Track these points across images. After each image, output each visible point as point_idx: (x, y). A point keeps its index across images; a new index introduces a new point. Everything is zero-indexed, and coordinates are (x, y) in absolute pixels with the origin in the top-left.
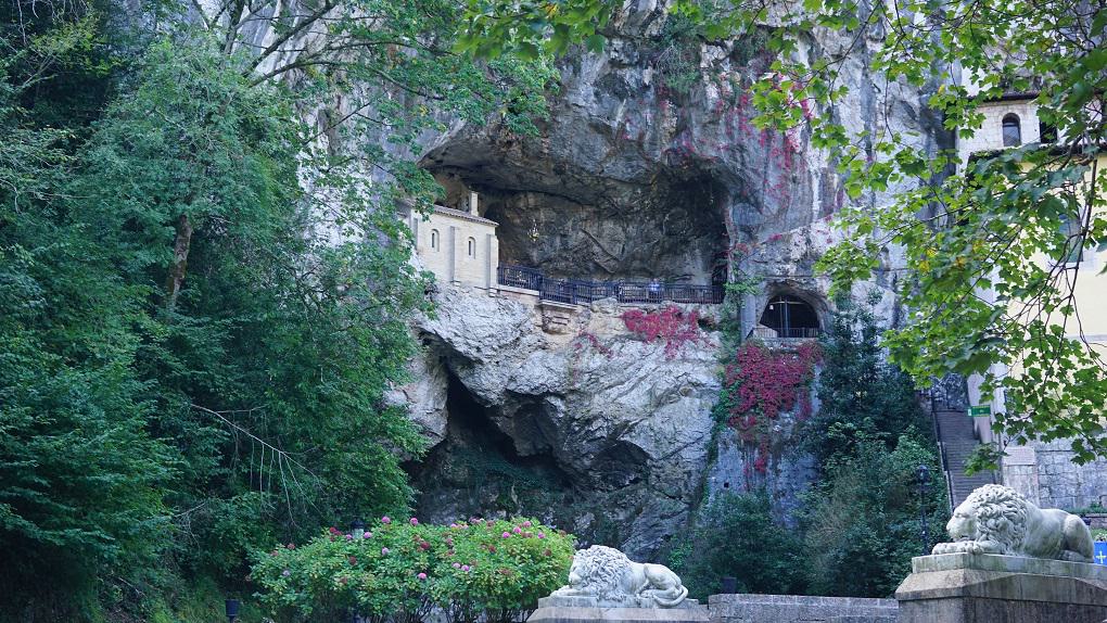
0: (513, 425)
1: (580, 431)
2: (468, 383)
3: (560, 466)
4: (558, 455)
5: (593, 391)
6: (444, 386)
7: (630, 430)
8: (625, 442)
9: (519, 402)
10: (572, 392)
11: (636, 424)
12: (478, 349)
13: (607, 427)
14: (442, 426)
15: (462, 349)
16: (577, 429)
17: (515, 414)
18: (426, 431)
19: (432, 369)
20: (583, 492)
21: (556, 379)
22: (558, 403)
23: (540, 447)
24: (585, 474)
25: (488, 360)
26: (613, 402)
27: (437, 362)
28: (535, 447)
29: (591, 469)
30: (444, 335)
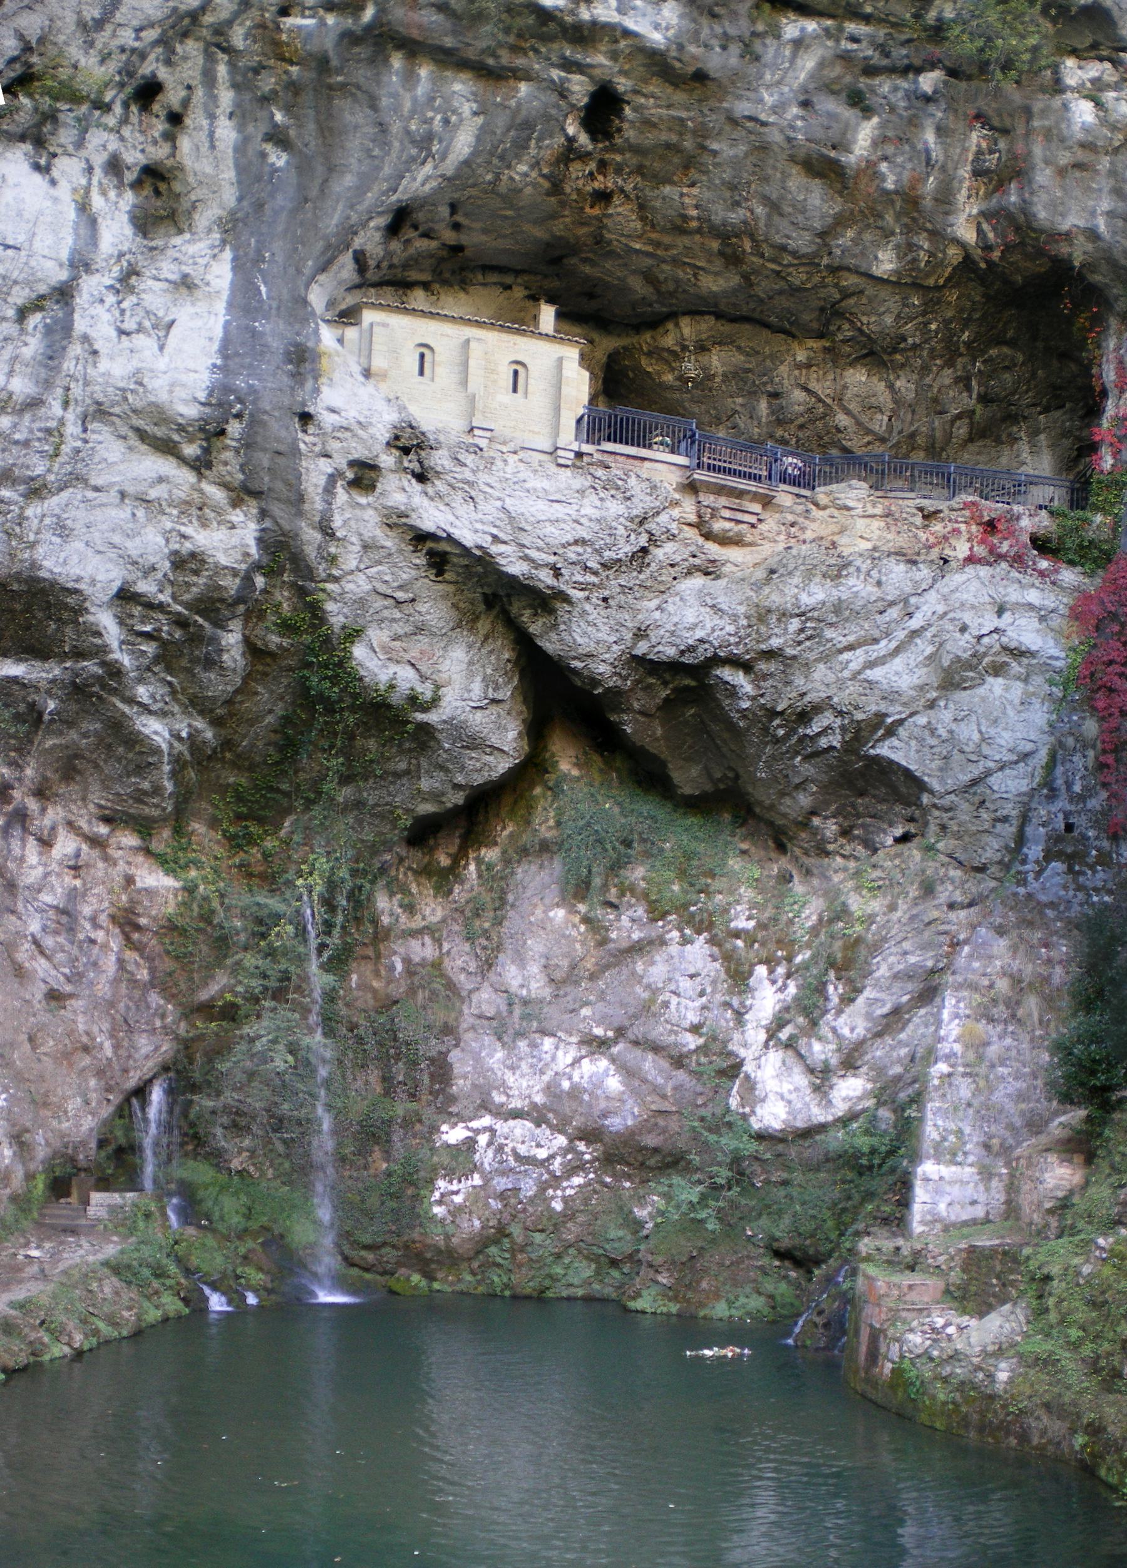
0: (659, 732)
2: (550, 645)
5: (812, 656)
6: (507, 656)
9: (665, 683)
10: (770, 654)
12: (557, 572)
14: (512, 735)
15: (516, 568)
17: (659, 709)
19: (476, 619)
21: (731, 629)
22: (739, 679)
25: (581, 595)
26: (854, 676)
27: (482, 607)
28: (709, 776)
30: (468, 538)
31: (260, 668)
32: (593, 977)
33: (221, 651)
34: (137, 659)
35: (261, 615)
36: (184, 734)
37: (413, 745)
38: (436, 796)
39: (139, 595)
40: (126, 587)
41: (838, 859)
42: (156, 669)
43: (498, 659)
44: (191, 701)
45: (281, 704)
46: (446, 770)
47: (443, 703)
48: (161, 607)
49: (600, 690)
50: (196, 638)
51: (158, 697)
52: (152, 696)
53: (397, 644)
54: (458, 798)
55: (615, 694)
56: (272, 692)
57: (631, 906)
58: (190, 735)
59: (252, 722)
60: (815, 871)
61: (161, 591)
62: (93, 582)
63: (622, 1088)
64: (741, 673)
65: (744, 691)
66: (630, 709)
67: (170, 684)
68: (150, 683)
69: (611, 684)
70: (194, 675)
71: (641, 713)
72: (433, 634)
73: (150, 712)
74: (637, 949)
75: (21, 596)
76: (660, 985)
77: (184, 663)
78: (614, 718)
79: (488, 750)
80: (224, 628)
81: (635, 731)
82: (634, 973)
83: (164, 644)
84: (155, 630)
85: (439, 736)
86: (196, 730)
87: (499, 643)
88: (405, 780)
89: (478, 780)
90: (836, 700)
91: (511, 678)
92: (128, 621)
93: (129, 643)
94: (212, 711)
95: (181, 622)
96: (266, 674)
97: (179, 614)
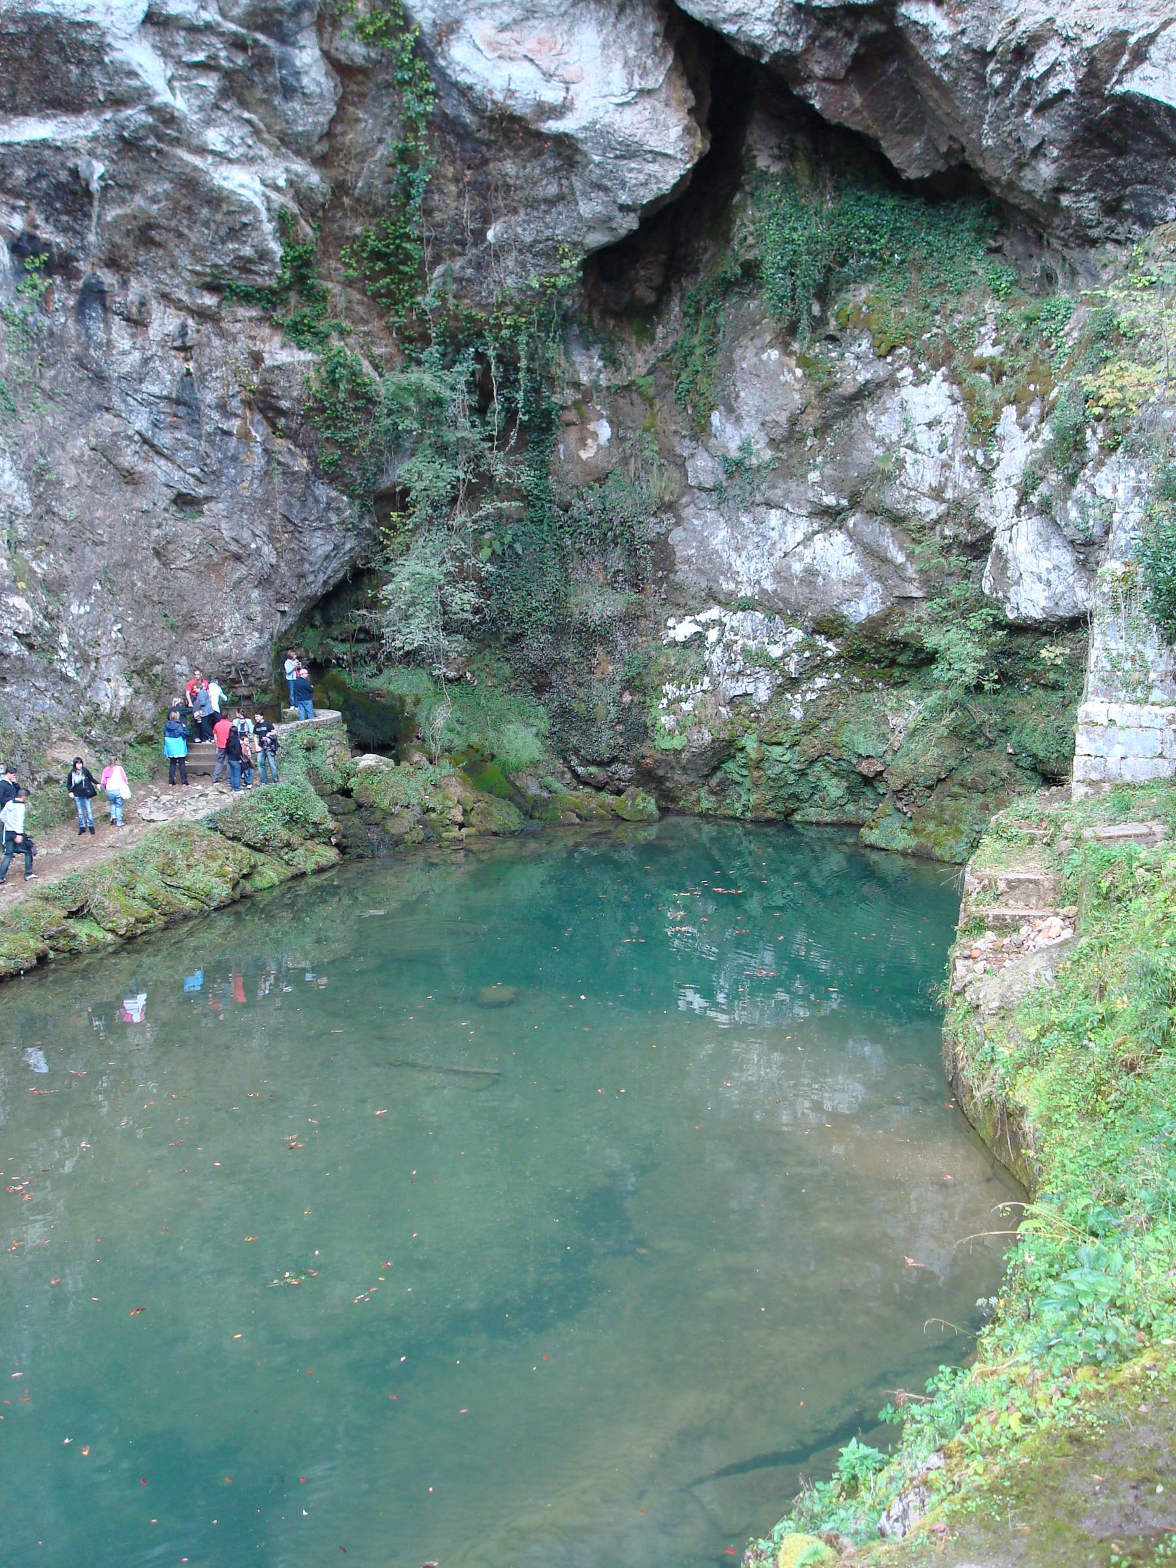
0: (858, 100)
1: (1007, 85)
3: (997, 191)
4: (980, 164)
6: (651, 28)
7: (1139, 56)
8: (1127, 100)
9: (849, 35)
11: (1151, 38)
13: (1075, 63)
14: (675, 132)
16: (998, 80)
17: (850, 70)
18: (631, 151)
20: (1066, 252)
23: (944, 149)
24: (1054, 207)
29: (1060, 190)
31: (355, 88)
32: (821, 431)
33: (297, 74)
34: (197, 97)
35: (336, 24)
36: (281, 183)
37: (559, 163)
38: (605, 222)
39: (177, 18)
40: (155, 9)
41: (1109, 247)
42: (226, 106)
43: (642, 34)
44: (282, 140)
45: (390, 131)
46: (606, 189)
47: (578, 104)
48: (209, 28)
49: (765, 60)
50: (263, 62)
51: (237, 141)
52: (228, 141)
53: (507, 36)
54: (629, 223)
55: (787, 59)
56: (375, 116)
57: (855, 339)
58: (290, 183)
59: (362, 156)
60: (1080, 269)
61: (204, 8)
62: (109, 10)
63: (859, 570)
64: (931, 6)
65: (938, 30)
66: (810, 78)
67: (249, 122)
68: (222, 125)
69: (777, 48)
70: (275, 108)
71: (826, 79)
72: (550, 16)
73: (230, 161)
74: (866, 393)
75: (23, 39)
76: (895, 438)
77: (259, 93)
78: (797, 91)
79: (649, 157)
80: (294, 45)
81: (826, 105)
82: (865, 425)
83: (227, 74)
84: (209, 57)
85: (584, 147)
86: (297, 175)
87: (640, 11)
88: (560, 207)
89: (646, 196)
90: (1059, 22)
91: (664, 56)
92: (173, 52)
93: (181, 78)
94: (310, 149)
95: (238, 44)
96: (362, 96)
97: (235, 34)
